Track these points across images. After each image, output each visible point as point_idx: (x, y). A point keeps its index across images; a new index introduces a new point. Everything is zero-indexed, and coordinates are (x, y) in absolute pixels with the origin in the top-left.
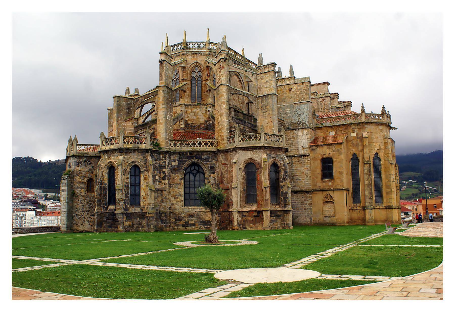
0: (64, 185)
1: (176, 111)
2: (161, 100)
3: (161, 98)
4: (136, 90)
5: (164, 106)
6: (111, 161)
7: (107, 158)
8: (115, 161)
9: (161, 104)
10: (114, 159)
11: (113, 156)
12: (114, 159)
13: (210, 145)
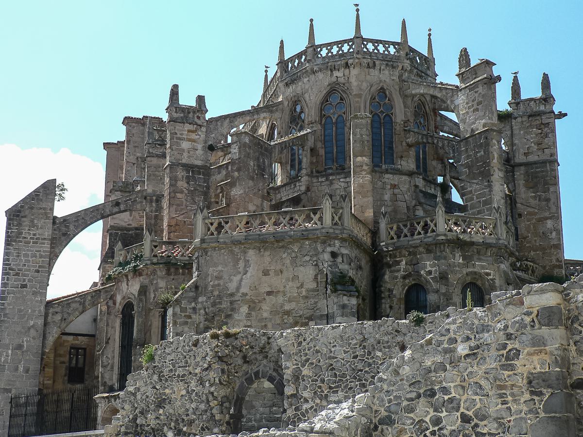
0: (348, 310)
1: (396, 183)
2: (495, 161)
3: (496, 156)
4: (201, 99)
5: (501, 174)
6: (475, 270)
7: (461, 261)
8: (488, 274)
9: (497, 170)
10: (483, 267)
11: (480, 260)
12: (483, 267)
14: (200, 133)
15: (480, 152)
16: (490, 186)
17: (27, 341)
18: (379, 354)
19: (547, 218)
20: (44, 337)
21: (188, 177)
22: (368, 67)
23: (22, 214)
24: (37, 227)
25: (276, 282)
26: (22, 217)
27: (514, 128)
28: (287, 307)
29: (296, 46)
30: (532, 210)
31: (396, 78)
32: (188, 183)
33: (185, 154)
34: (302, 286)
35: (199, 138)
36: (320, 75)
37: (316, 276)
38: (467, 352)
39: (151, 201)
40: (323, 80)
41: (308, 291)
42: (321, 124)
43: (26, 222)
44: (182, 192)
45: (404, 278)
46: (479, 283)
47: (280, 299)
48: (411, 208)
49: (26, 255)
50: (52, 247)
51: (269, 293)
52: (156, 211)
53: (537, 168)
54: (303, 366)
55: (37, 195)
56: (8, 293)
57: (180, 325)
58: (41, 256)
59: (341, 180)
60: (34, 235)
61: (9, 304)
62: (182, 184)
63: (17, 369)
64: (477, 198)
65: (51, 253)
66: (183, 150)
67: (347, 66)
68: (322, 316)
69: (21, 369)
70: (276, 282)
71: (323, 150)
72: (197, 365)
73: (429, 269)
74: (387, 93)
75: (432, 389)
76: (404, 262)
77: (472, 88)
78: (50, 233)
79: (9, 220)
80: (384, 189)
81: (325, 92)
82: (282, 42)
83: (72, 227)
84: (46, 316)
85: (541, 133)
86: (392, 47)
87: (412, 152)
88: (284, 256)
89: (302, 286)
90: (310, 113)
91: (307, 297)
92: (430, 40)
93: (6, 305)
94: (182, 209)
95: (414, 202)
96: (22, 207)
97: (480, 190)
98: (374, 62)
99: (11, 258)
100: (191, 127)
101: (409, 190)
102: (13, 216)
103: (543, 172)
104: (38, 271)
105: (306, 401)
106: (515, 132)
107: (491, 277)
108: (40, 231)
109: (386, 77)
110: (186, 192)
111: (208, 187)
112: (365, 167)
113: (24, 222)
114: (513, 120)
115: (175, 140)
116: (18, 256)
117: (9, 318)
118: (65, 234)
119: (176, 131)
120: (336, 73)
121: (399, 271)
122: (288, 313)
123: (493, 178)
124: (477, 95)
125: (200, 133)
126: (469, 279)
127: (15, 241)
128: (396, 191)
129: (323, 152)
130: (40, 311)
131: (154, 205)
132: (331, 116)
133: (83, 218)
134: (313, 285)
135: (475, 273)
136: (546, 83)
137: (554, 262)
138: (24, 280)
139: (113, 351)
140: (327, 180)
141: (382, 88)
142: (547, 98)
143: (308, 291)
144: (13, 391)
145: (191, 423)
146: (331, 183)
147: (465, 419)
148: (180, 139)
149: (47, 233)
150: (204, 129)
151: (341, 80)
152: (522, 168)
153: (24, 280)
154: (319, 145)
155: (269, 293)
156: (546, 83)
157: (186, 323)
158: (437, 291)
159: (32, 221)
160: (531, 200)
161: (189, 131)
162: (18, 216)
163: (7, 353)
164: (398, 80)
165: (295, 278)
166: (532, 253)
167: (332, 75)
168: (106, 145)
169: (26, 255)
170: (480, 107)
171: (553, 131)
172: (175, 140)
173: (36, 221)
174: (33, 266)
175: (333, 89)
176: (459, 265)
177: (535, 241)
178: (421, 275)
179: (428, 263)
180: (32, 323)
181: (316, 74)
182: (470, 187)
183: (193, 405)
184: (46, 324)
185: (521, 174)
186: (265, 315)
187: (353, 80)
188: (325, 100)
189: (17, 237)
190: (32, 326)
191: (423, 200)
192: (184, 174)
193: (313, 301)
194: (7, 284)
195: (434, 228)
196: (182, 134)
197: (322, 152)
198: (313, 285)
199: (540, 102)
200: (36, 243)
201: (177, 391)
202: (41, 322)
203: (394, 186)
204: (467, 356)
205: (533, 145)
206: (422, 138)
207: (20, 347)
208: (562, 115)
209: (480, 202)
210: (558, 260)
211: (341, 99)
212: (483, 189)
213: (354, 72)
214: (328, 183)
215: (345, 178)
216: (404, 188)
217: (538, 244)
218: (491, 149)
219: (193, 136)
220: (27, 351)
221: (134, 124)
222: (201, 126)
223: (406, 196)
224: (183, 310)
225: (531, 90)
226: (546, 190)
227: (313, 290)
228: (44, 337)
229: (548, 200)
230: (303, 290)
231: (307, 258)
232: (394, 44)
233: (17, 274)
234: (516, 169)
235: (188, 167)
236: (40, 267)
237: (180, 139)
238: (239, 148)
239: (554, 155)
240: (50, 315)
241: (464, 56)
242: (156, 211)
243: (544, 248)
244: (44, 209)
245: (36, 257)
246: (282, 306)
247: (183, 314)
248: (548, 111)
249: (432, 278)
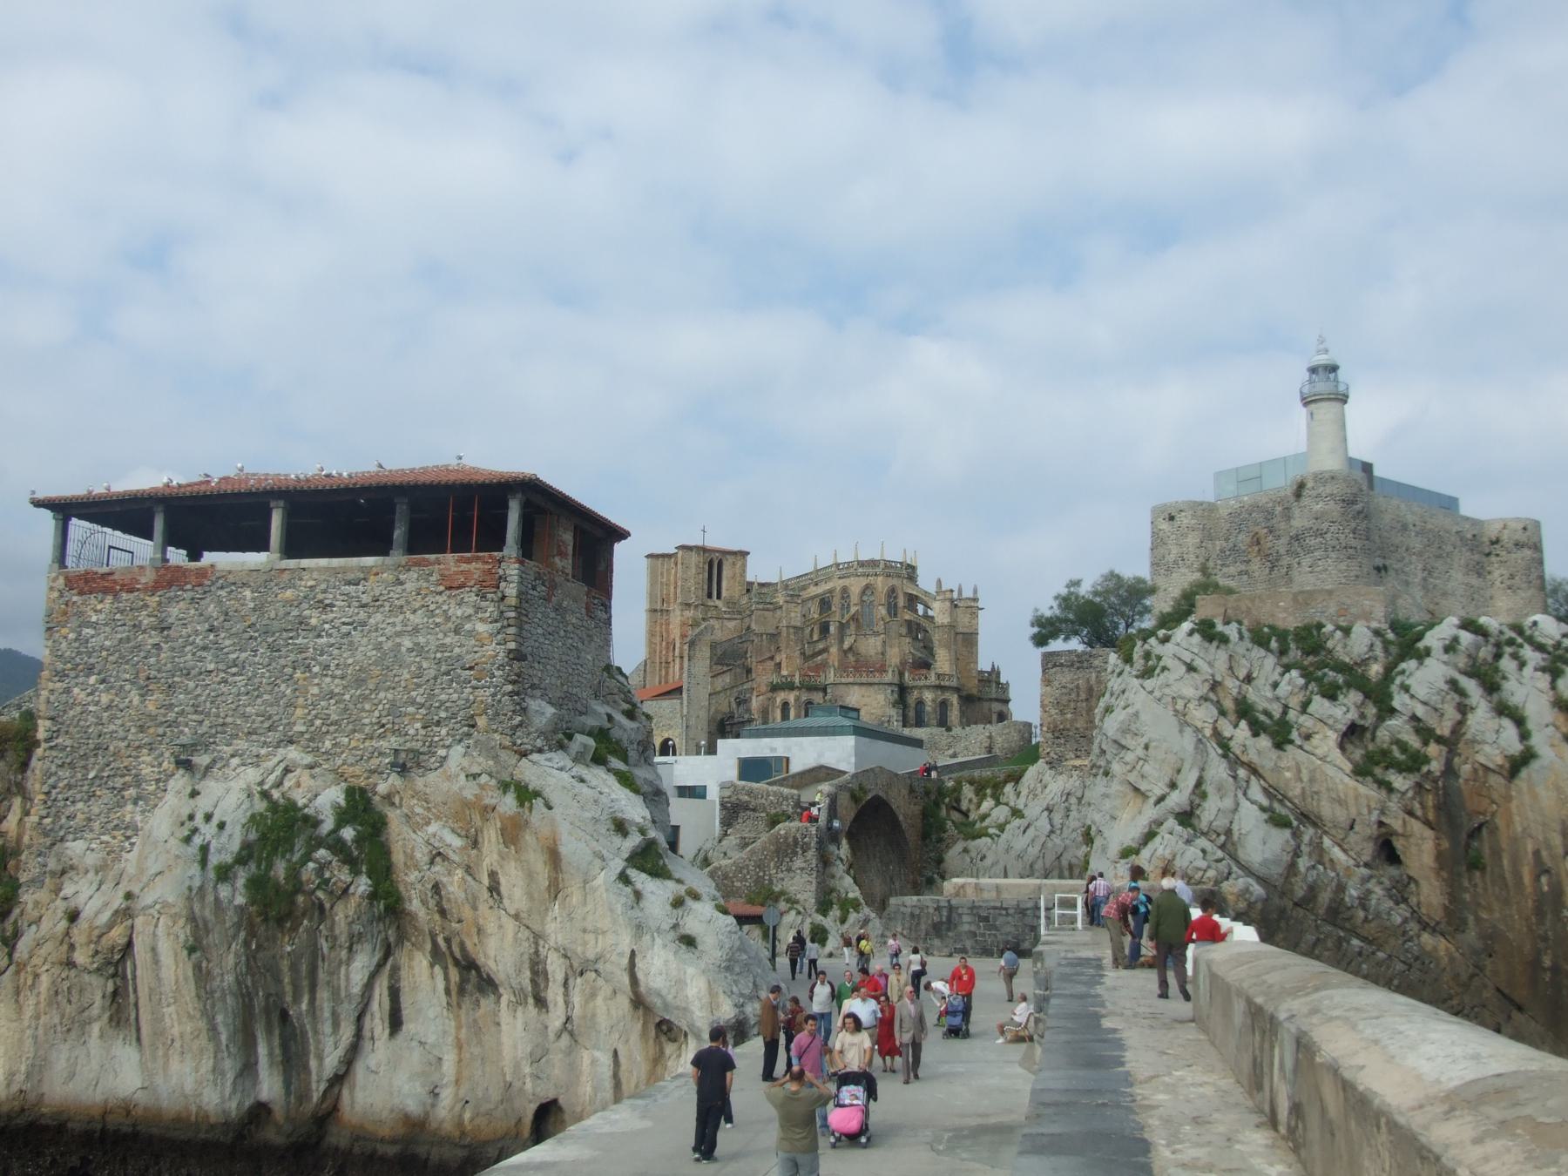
20: (709, 710)
25: (866, 700)
43: (697, 648)
62: (792, 637)
67: (876, 575)
70: (866, 700)
90: (854, 598)
136: (975, 591)
142: (975, 600)
156: (975, 591)
175: (867, 587)
188: (863, 593)
213: (880, 578)
225: (968, 593)
228: (709, 710)
235: (794, 627)
239: (977, 629)
241: (939, 582)
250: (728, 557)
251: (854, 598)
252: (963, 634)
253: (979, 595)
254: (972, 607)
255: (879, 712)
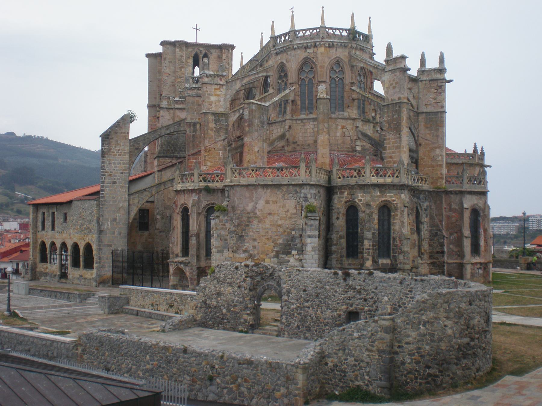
0: (313, 228)
1: (345, 125)
2: (404, 121)
6: (387, 199)
7: (378, 194)
8: (394, 201)
9: (404, 127)
10: (391, 197)
11: (389, 193)
13: (375, 175)
14: (222, 90)
15: (395, 115)
16: (400, 138)
17: (119, 216)
18: (327, 287)
19: (436, 148)
20: (129, 213)
21: (215, 120)
22: (329, 47)
23: (110, 137)
24: (120, 145)
25: (273, 207)
26: (111, 139)
27: (420, 87)
28: (280, 222)
29: (282, 28)
30: (427, 142)
31: (346, 54)
32: (215, 124)
33: (213, 105)
34: (288, 211)
35: (221, 94)
36: (298, 52)
37: (296, 206)
38: (357, 336)
39: (190, 126)
40: (302, 55)
41: (291, 214)
42: (298, 84)
43: (113, 142)
44: (212, 130)
45: (346, 202)
46: (389, 206)
47: (276, 218)
48: (354, 140)
49: (115, 163)
50: (130, 157)
51: (270, 214)
52: (193, 132)
53: (432, 115)
54: (292, 288)
55: (118, 124)
56: (106, 187)
57: (219, 230)
58: (124, 164)
59: (311, 123)
60: (119, 150)
61: (107, 194)
63: (114, 233)
64: (392, 144)
65: (129, 161)
66: (212, 102)
67: (315, 46)
68: (299, 229)
69: (117, 233)
70: (273, 207)
71: (300, 101)
72: (238, 279)
73: (360, 198)
74: (341, 65)
75: (345, 348)
76: (346, 193)
77: (393, 71)
78: (129, 148)
79: (103, 141)
80: (337, 129)
81: (301, 63)
82: (273, 22)
83: (141, 144)
84: (129, 201)
85: (436, 92)
86: (344, 31)
87: (356, 103)
88: (278, 193)
89: (288, 211)
90: (292, 77)
91: (290, 218)
92: (370, 21)
93: (105, 195)
94: (212, 141)
95: (355, 137)
96: (110, 132)
97: (394, 139)
98: (333, 44)
99: (105, 165)
100: (216, 87)
101: (352, 129)
102: (105, 138)
103: (435, 118)
104: (122, 173)
105: (293, 304)
106: (420, 90)
107: (395, 202)
108: (122, 147)
109: (341, 54)
110: (214, 129)
111: (228, 126)
112: (325, 130)
113: (112, 142)
114: (420, 83)
115: (207, 96)
116: (110, 164)
117: (107, 202)
118: (137, 149)
119: (207, 90)
120: (308, 50)
121: (343, 197)
122: (280, 226)
123: (402, 133)
124: (395, 77)
125: (222, 90)
126: (382, 204)
127: (107, 154)
128: (345, 130)
129: (300, 104)
130: (125, 197)
131: (192, 128)
132: (305, 79)
133: (148, 138)
134: (294, 211)
135: (386, 200)
136: (442, 60)
137: (439, 175)
138: (114, 179)
139: (177, 234)
140: (302, 122)
141: (337, 61)
142: (441, 70)
143: (291, 214)
144: (113, 246)
145: (235, 306)
146: (304, 125)
147: (356, 360)
148: (209, 95)
149: (127, 148)
150: (224, 87)
151: (312, 55)
152: (424, 115)
153: (114, 179)
154: (297, 98)
155: (270, 214)
156: (442, 60)
157: (222, 228)
158: (364, 212)
159: (117, 141)
160: (428, 136)
161: (215, 89)
162: (108, 138)
163: (108, 223)
164: (348, 55)
165: (284, 206)
166: (426, 169)
167: (305, 52)
168: (148, 56)
169: (115, 163)
170: (397, 85)
171: (444, 91)
172: (207, 96)
173: (119, 142)
174: (119, 170)
176: (377, 196)
177: (429, 161)
178: (355, 202)
179: (360, 195)
180: (121, 205)
181: (296, 50)
182: (389, 136)
183: (237, 298)
184: (129, 205)
185: (422, 118)
186: (268, 226)
187: (319, 56)
188: (301, 69)
189: (109, 152)
190: (121, 207)
191: (361, 137)
192: (213, 117)
193: (294, 220)
194: (105, 181)
195: (364, 175)
196: (211, 92)
197: (299, 103)
198: (294, 211)
199: (437, 71)
200: (120, 155)
201: (227, 290)
202: (126, 204)
203: (343, 127)
204: (357, 338)
205: (431, 99)
206: (362, 97)
207: (115, 220)
208: (450, 81)
209: (394, 146)
210: (441, 174)
211: (312, 68)
212: (396, 139)
213: (321, 50)
214: (302, 124)
215: (313, 122)
216: (349, 127)
217: (430, 164)
218: (402, 115)
219: (218, 92)
220: (119, 222)
221: (168, 46)
222: (222, 85)
223: (350, 133)
224: (221, 221)
225: (432, 63)
226: (437, 130)
227: (294, 214)
228: (129, 213)
229: (437, 136)
230: (289, 213)
231: (291, 195)
232: (346, 30)
233: (110, 175)
234: (420, 115)
236: (123, 170)
237: (209, 95)
238: (249, 112)
239: (443, 107)
240: (131, 200)
241: (389, 50)
242: (193, 132)
243: (433, 166)
244: (124, 133)
245: (120, 163)
246: (277, 221)
247: (221, 224)
248: (442, 78)
249: (362, 204)
250: (213, 51)
251: (292, 77)
252: (426, 113)
253: (446, 65)
254: (437, 80)
255: (288, 224)
